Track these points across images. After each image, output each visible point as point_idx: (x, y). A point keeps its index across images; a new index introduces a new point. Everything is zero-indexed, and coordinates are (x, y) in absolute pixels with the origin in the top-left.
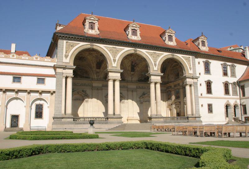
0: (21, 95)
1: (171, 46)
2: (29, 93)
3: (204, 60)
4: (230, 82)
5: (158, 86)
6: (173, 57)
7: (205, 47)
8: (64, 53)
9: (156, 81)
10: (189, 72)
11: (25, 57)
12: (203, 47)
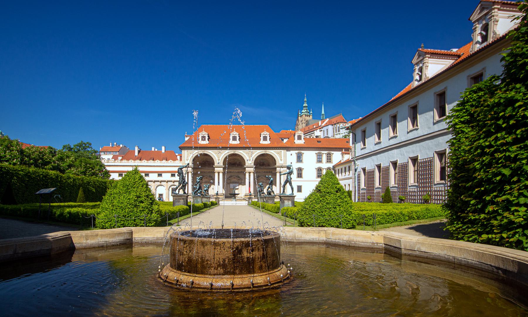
0: (162, 183)
1: (265, 145)
2: (167, 182)
3: (297, 152)
4: (323, 167)
5: (252, 174)
6: (265, 153)
7: (300, 140)
8: (186, 158)
9: (249, 171)
10: (279, 162)
11: (164, 161)
12: (298, 141)
